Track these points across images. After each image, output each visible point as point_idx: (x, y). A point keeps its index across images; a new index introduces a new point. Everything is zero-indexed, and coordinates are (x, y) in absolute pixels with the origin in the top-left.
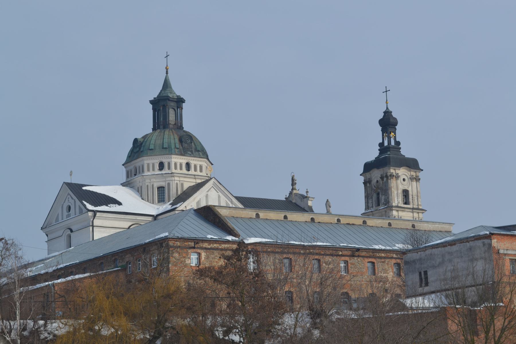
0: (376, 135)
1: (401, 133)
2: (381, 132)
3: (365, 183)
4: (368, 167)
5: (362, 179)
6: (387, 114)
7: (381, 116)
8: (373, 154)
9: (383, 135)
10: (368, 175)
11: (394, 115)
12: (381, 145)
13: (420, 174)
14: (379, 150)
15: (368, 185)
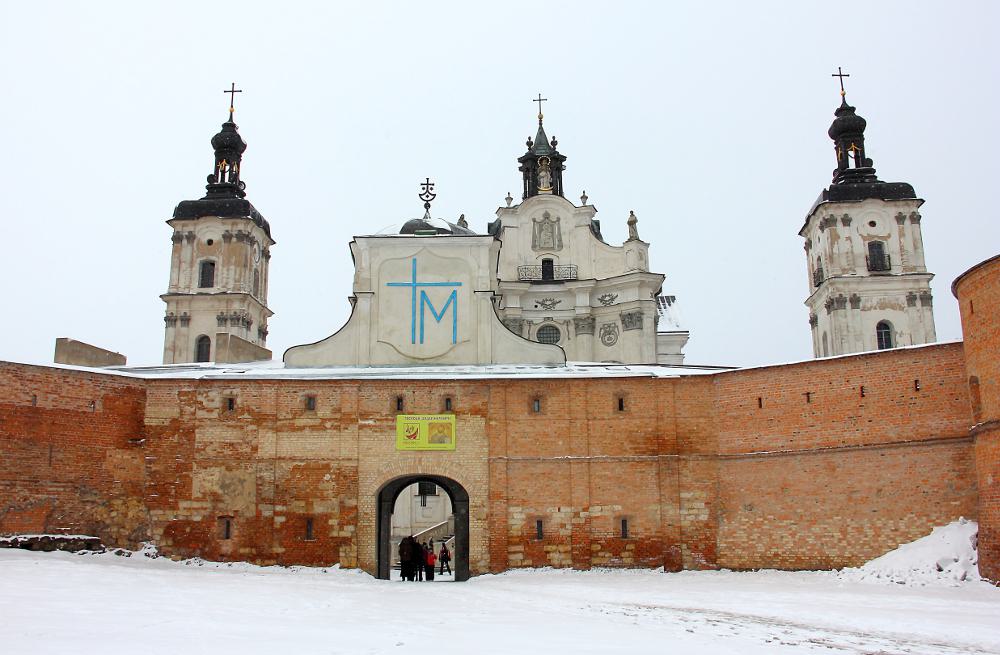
0: (207, 162)
1: (249, 169)
2: (213, 159)
3: (177, 238)
4: (186, 212)
5: (170, 231)
6: (230, 127)
7: (219, 130)
8: (198, 192)
9: (217, 163)
10: (188, 227)
11: (243, 132)
12: (211, 178)
13: (272, 248)
14: (207, 187)
15: (185, 242)
